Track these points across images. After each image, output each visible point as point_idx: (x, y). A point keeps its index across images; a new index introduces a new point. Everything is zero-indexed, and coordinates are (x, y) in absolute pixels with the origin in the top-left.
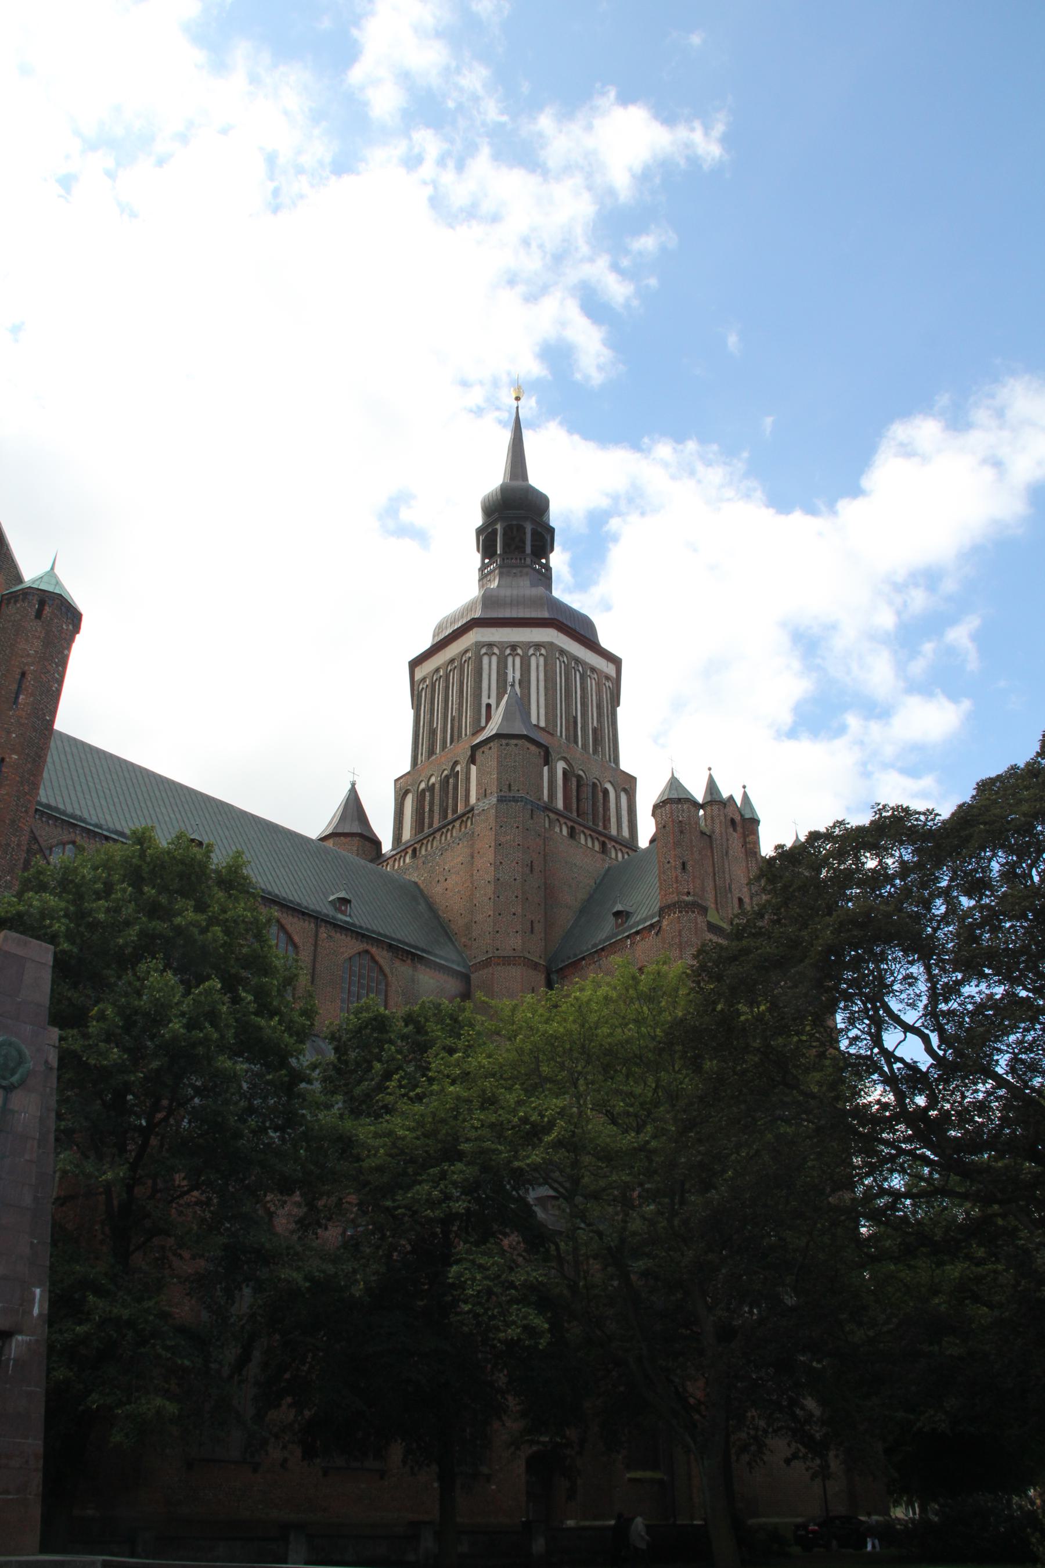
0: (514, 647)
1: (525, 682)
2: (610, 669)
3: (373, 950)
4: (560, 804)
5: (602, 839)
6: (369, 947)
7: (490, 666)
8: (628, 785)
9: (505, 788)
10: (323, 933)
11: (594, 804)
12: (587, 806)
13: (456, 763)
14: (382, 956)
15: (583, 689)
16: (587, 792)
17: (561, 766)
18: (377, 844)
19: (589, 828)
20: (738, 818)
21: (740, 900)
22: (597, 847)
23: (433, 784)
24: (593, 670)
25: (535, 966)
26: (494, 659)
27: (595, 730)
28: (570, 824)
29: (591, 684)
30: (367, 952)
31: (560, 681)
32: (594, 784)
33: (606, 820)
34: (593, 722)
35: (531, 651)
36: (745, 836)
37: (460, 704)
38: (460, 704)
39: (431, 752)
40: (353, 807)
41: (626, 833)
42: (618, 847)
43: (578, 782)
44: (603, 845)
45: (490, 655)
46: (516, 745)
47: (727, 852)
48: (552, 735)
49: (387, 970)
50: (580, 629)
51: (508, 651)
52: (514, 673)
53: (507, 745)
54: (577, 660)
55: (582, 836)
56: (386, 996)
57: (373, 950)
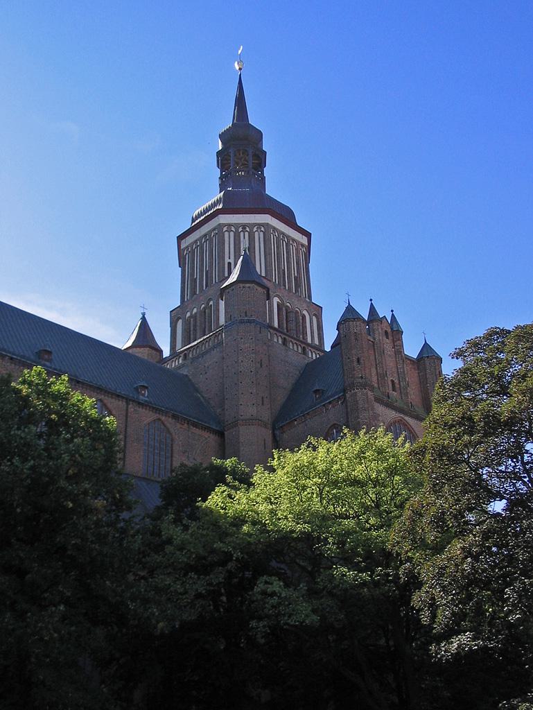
0: (244, 226)
1: (251, 247)
2: (304, 240)
3: (163, 418)
4: (276, 325)
5: (303, 346)
6: (160, 417)
7: (229, 238)
8: (317, 311)
9: (243, 315)
10: (131, 408)
11: (297, 323)
12: (292, 326)
13: (210, 300)
14: (169, 422)
16: (292, 316)
17: (276, 300)
18: (161, 352)
19: (295, 339)
20: (389, 330)
21: (392, 381)
22: (300, 350)
23: (196, 313)
24: (294, 240)
25: (266, 426)
26: (232, 234)
28: (283, 336)
30: (159, 419)
31: (273, 247)
32: (297, 312)
33: (304, 333)
34: (294, 273)
35: (255, 229)
36: (394, 342)
37: (211, 263)
38: (211, 263)
39: (194, 293)
41: (317, 342)
42: (313, 350)
43: (286, 310)
44: (304, 349)
45: (229, 231)
46: (249, 287)
47: (383, 353)
48: (270, 281)
49: (172, 430)
50: (286, 215)
51: (240, 229)
52: (244, 244)
53: (244, 287)
55: (291, 343)
56: (172, 447)
57: (163, 418)
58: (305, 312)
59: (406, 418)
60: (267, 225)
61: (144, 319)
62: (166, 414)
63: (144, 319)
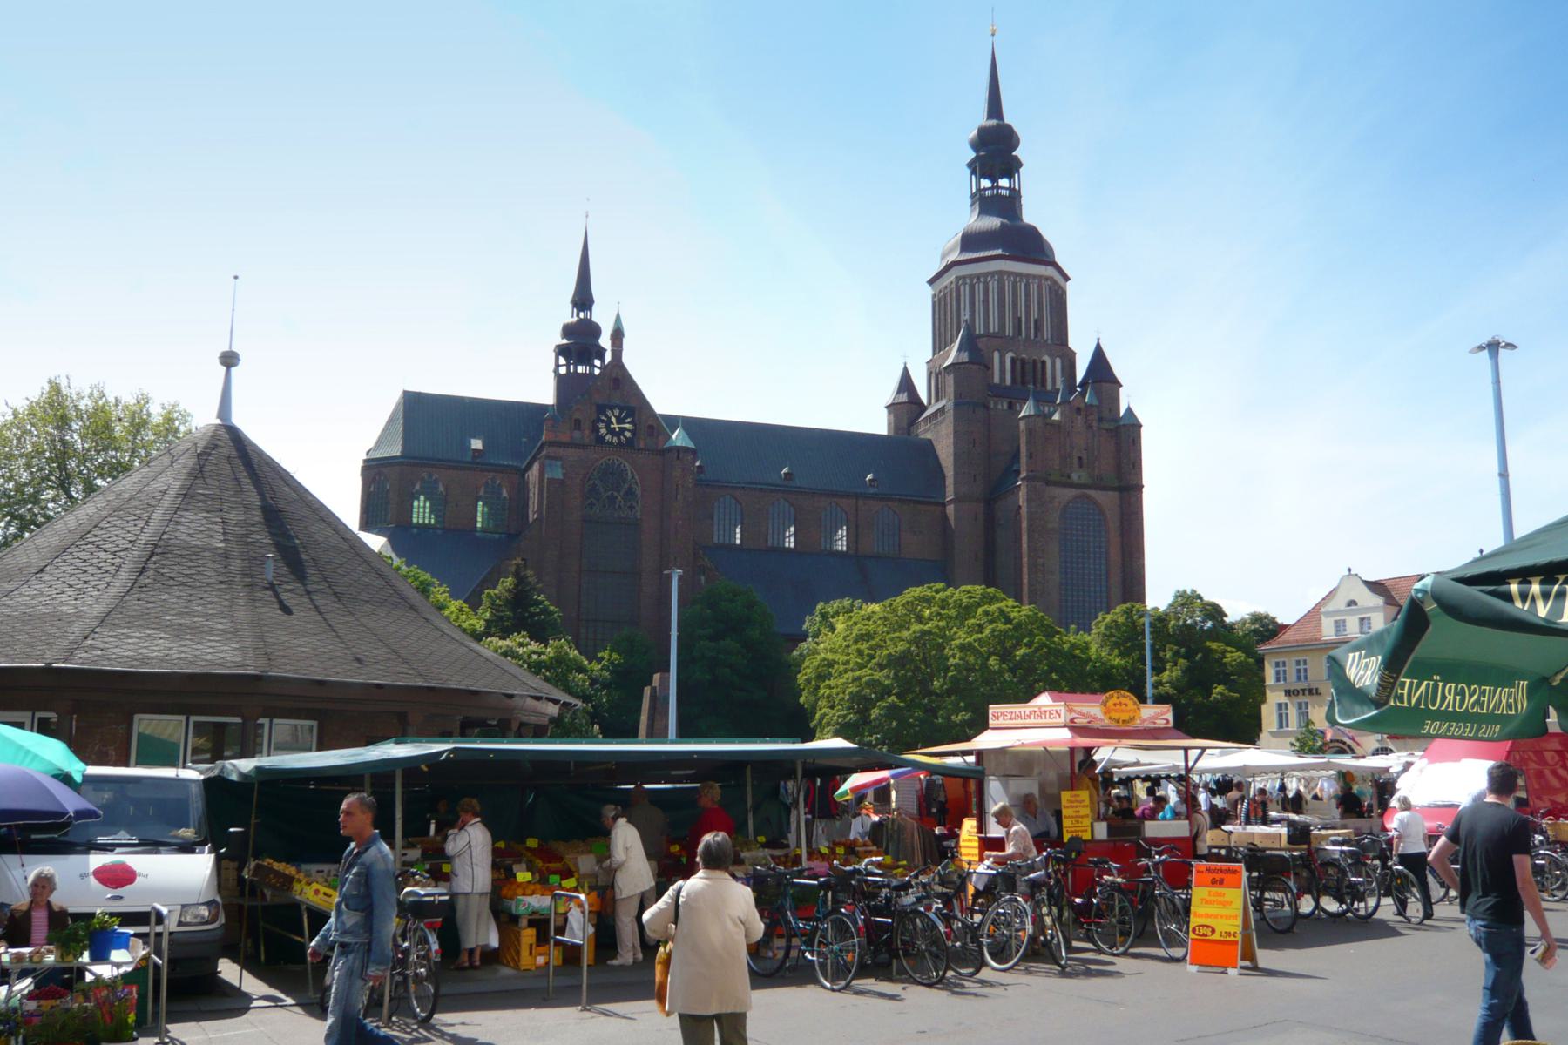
0: (978, 277)
10: (861, 502)
12: (1029, 376)
15: (1027, 295)
16: (1029, 368)
24: (1034, 277)
27: (1036, 321)
29: (1034, 288)
34: (1034, 315)
40: (906, 383)
52: (979, 296)
54: (1021, 275)
58: (1047, 358)
59: (1092, 493)
60: (1001, 273)
61: (906, 370)
62: (889, 500)
63: (906, 370)
